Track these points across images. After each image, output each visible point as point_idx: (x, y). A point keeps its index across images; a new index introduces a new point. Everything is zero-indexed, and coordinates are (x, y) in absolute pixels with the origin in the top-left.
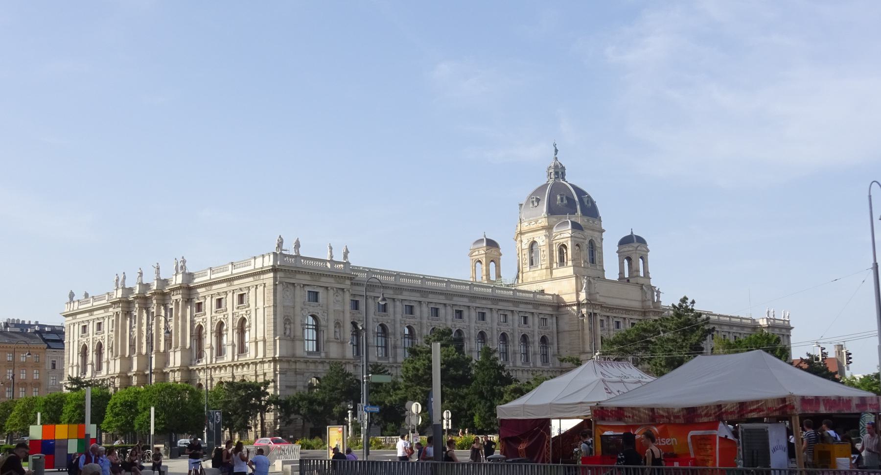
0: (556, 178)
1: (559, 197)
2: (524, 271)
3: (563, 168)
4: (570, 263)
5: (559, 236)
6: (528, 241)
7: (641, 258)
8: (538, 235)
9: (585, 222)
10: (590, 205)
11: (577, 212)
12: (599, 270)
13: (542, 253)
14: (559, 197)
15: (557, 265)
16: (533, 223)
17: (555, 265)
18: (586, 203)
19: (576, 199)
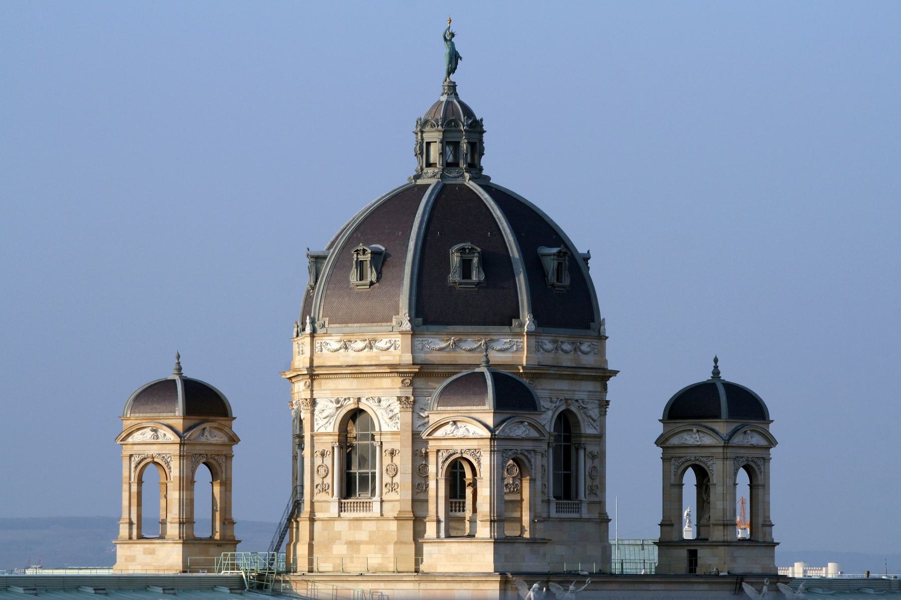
0: (448, 165)
1: (455, 259)
2: (318, 515)
3: (476, 127)
4: (484, 531)
5: (448, 428)
6: (338, 408)
7: (747, 468)
8: (377, 394)
9: (547, 351)
10: (566, 281)
11: (518, 317)
12: (589, 520)
13: (387, 460)
14: (455, 259)
15: (438, 532)
16: (360, 345)
17: (431, 529)
18: (552, 278)
19: (514, 252)
